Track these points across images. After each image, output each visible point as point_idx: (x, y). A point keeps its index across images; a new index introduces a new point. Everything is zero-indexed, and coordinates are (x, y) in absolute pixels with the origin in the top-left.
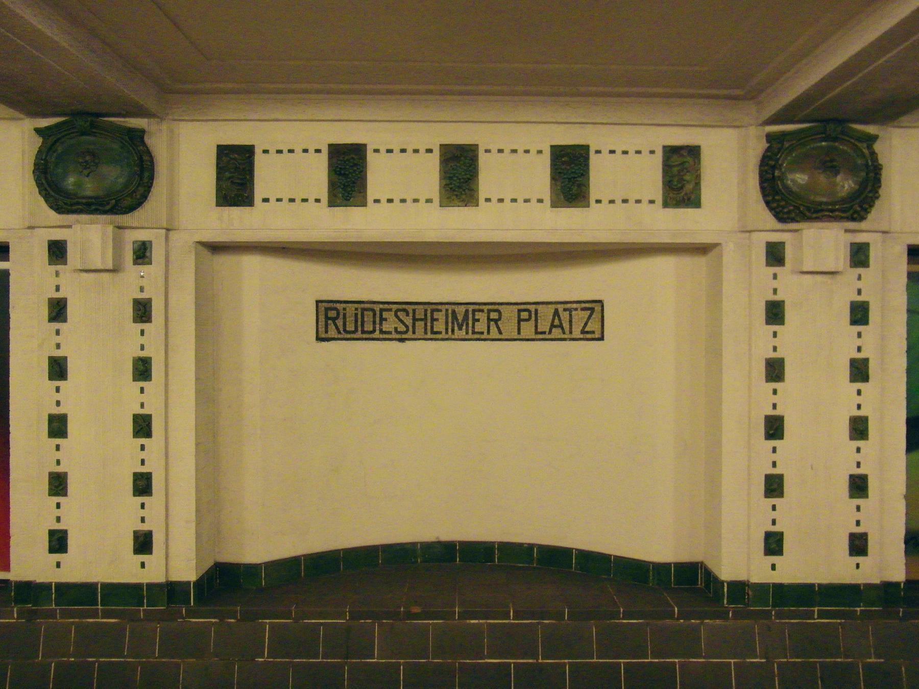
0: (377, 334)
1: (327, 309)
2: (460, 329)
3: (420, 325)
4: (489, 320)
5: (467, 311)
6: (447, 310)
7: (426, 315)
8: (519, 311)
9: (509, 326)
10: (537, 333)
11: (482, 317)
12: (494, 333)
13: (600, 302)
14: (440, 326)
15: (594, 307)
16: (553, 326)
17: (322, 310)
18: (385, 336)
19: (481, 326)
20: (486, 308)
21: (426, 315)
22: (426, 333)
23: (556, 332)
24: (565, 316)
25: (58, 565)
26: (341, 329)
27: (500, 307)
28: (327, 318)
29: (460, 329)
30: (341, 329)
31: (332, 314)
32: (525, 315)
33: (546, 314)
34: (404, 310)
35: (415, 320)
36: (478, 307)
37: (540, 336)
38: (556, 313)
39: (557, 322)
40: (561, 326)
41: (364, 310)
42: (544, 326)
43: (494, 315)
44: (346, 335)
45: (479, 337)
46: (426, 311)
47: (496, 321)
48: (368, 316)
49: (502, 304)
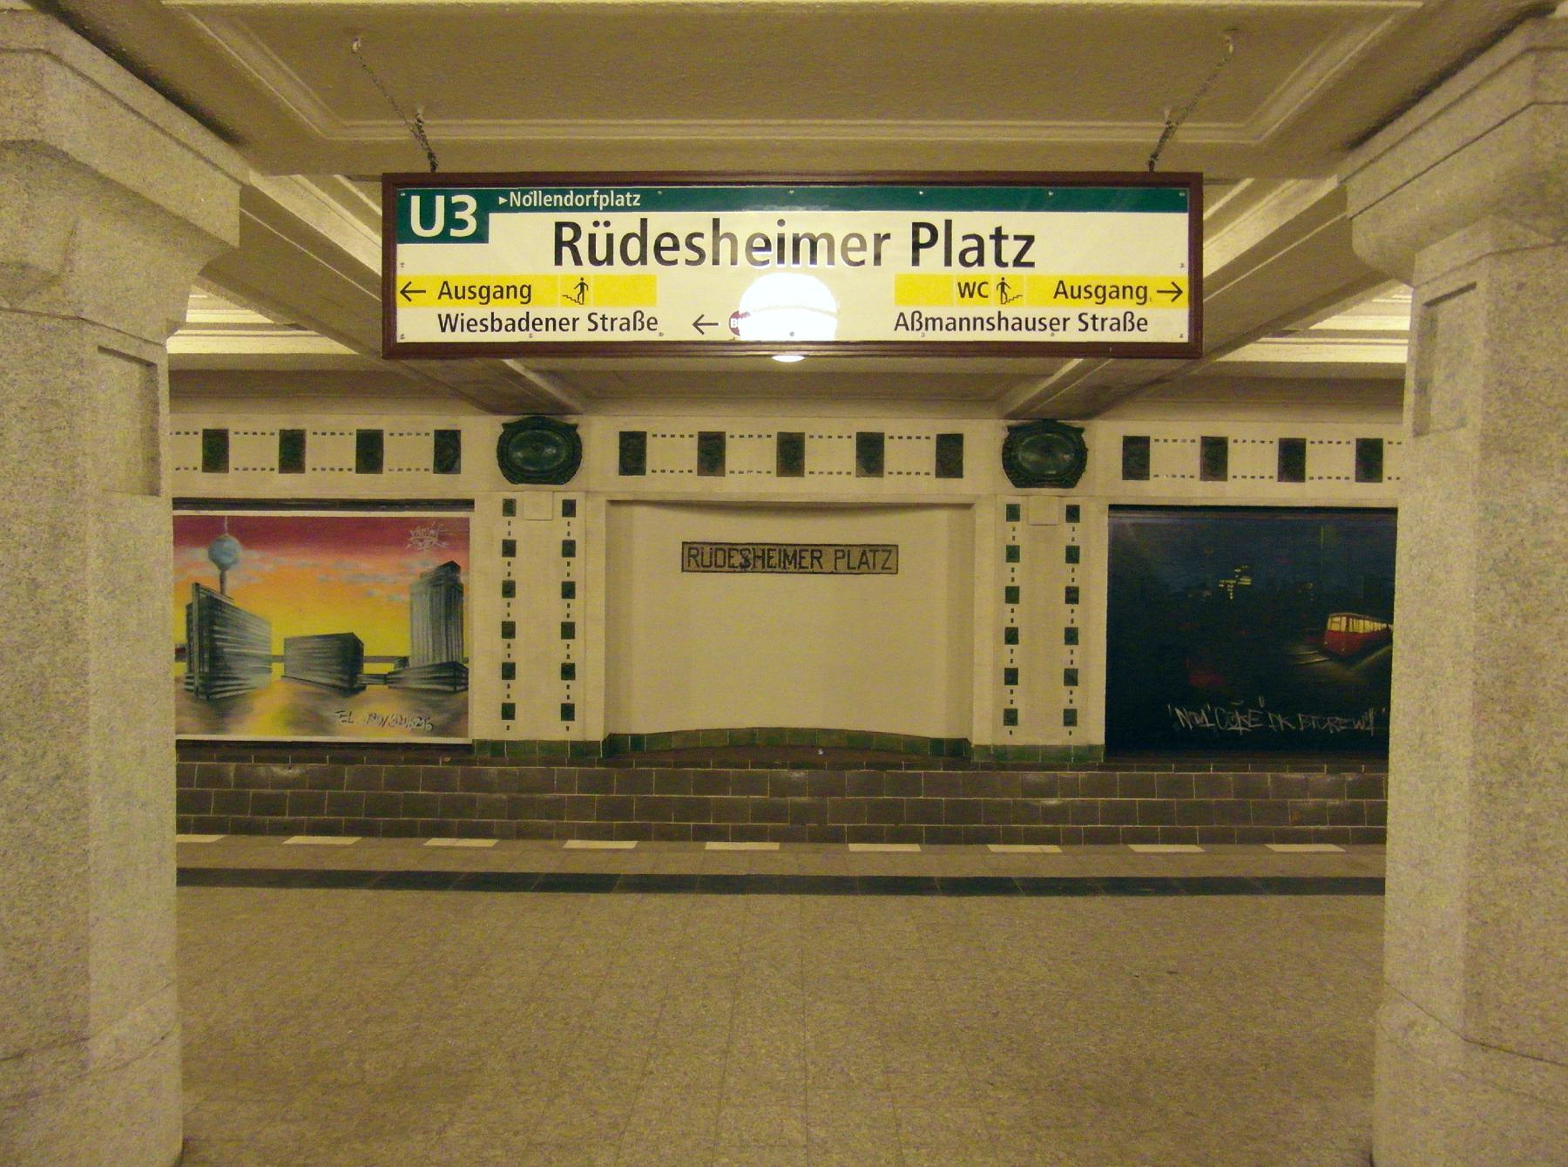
0: (726, 568)
1: (690, 549)
2: (790, 563)
3: (759, 563)
4: (813, 557)
5: (795, 551)
6: (780, 550)
7: (764, 554)
8: (836, 551)
9: (828, 561)
10: (849, 567)
11: (807, 555)
12: (817, 568)
13: (896, 546)
14: (774, 561)
15: (890, 550)
16: (861, 563)
17: (686, 549)
18: (733, 569)
19: (806, 562)
20: (810, 548)
21: (764, 554)
22: (763, 567)
23: (864, 567)
24: (870, 555)
25: (508, 728)
26: (700, 562)
27: (820, 548)
28: (690, 556)
29: (790, 563)
30: (700, 562)
31: (694, 552)
32: (840, 554)
33: (856, 554)
34: (747, 549)
35: (755, 557)
36: (803, 548)
37: (851, 570)
38: (864, 554)
39: (864, 560)
40: (867, 563)
41: (717, 550)
42: (855, 562)
43: (817, 554)
44: (705, 568)
45: (802, 570)
46: (763, 551)
47: (818, 559)
48: (720, 554)
49: (821, 545)
